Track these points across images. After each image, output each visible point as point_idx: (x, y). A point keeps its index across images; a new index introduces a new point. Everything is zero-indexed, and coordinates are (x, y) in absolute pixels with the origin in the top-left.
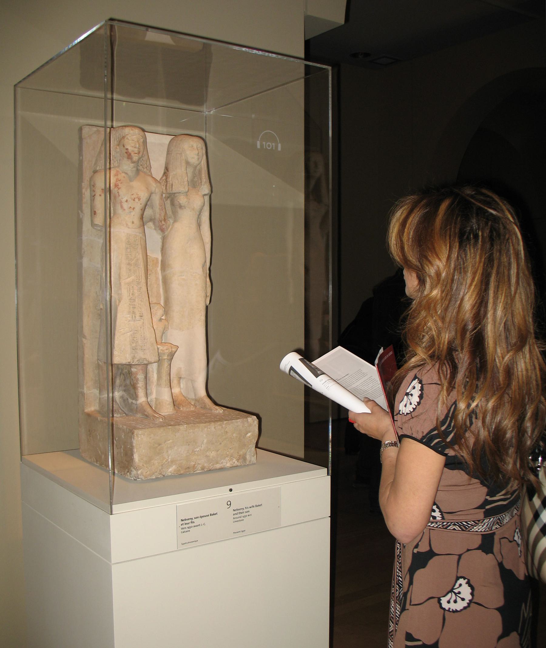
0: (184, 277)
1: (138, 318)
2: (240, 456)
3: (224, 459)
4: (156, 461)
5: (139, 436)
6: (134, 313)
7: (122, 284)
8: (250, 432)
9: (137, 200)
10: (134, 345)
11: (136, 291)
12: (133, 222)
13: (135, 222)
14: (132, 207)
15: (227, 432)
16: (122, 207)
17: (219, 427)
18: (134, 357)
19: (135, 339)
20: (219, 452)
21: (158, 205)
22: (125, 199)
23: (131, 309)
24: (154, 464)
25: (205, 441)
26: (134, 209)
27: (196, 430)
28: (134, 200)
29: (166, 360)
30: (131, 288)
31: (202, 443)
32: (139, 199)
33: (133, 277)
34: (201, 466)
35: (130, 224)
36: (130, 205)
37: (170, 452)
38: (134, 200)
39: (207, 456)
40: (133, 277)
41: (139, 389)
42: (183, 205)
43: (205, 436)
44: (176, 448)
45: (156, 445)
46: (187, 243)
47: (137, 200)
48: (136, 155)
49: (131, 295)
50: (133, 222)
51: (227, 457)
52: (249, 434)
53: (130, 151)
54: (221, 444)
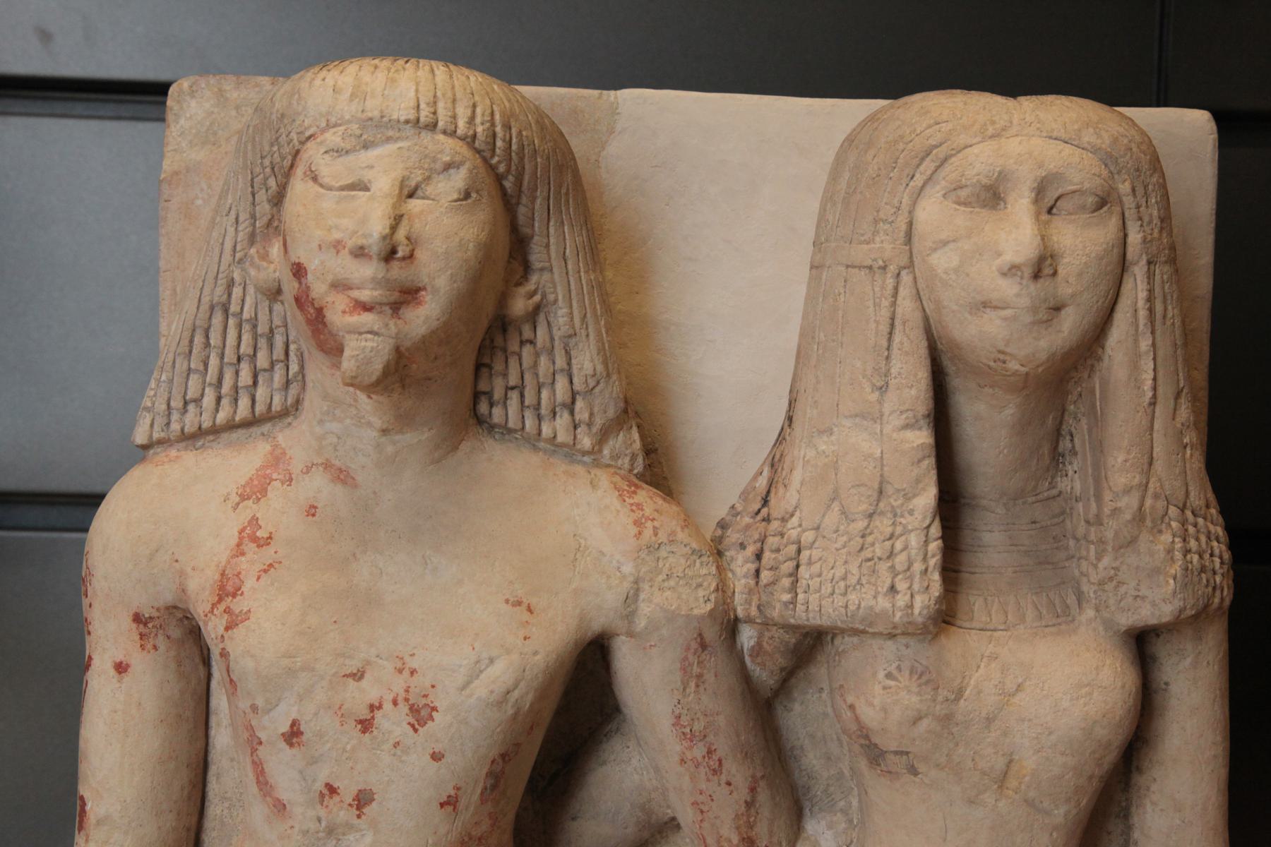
9: (393, 723)
14: (348, 790)
21: (664, 725)
26: (362, 800)
28: (366, 725)
32: (420, 715)
36: (323, 774)
38: (366, 725)
42: (889, 743)
47: (393, 723)
48: (367, 319)
53: (318, 289)
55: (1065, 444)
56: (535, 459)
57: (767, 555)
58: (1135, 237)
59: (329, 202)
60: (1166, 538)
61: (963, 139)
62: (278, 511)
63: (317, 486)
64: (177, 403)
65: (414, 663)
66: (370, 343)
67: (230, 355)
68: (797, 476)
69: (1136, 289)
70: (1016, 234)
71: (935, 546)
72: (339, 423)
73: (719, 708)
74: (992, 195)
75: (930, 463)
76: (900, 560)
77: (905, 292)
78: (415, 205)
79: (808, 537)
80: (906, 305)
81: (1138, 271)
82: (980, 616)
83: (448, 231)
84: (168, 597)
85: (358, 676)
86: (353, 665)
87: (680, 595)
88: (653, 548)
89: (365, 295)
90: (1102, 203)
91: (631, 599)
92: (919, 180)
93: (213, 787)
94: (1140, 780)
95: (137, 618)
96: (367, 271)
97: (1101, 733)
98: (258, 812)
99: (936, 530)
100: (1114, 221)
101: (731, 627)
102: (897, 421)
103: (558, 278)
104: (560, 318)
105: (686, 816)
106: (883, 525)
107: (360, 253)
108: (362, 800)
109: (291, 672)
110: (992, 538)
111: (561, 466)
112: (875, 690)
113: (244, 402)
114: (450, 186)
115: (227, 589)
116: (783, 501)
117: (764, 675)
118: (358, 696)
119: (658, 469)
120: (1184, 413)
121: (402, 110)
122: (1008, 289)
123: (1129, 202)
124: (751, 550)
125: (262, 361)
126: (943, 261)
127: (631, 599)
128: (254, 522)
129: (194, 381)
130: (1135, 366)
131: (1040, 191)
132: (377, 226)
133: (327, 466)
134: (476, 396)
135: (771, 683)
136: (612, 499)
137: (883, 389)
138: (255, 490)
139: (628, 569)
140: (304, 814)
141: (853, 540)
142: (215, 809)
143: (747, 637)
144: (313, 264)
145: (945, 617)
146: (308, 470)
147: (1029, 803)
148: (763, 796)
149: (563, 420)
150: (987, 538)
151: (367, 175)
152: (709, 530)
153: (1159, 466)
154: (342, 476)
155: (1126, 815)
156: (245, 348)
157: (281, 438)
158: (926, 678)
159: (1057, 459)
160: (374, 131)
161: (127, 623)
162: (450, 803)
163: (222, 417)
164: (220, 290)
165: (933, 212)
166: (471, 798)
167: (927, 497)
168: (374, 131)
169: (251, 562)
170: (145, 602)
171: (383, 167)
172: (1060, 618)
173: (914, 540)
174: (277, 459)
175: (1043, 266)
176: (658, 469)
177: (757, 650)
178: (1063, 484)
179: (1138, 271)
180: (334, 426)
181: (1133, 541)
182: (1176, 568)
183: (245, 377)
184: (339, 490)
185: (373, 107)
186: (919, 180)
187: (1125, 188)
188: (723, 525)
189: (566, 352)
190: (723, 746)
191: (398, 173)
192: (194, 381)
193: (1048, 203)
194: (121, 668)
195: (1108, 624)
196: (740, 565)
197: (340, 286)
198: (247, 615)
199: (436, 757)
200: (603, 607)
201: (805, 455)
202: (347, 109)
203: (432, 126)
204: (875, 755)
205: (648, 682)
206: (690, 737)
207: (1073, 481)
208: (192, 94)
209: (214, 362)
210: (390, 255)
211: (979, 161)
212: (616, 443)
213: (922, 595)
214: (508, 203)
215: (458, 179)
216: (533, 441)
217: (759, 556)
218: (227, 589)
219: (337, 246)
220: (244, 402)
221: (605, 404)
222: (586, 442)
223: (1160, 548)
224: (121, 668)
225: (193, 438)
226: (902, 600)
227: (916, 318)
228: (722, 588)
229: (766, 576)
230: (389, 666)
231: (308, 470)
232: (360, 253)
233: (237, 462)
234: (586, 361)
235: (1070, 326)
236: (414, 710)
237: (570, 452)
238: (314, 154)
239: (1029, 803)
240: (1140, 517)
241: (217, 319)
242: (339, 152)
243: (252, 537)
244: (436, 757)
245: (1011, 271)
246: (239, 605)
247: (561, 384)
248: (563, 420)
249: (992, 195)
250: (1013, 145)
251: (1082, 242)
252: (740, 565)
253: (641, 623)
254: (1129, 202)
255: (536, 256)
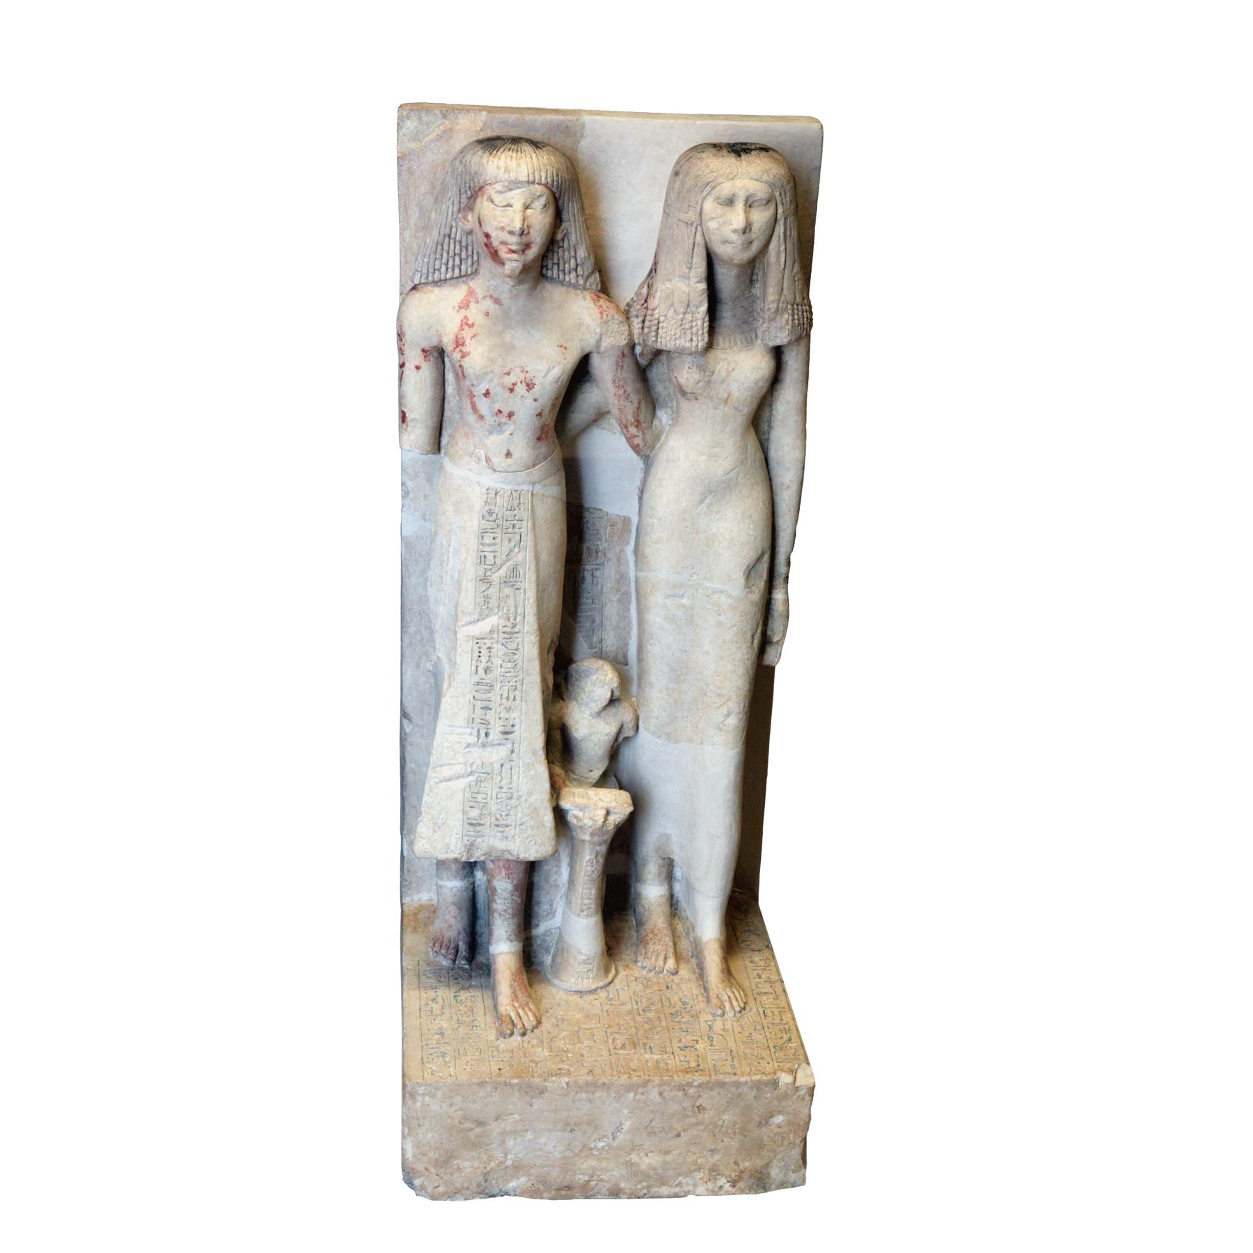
0: (685, 601)
1: (495, 735)
2: (741, 1172)
3: (689, 1173)
4: (467, 1164)
5: (420, 1098)
6: (485, 723)
7: (459, 636)
8: (780, 1112)
9: (521, 389)
10: (474, 813)
11: (497, 662)
12: (508, 454)
13: (516, 455)
14: (506, 411)
15: (700, 1108)
16: (475, 409)
17: (674, 1093)
18: (472, 845)
19: (480, 797)
20: (669, 1158)
22: (482, 389)
23: (478, 711)
24: (459, 1169)
25: (627, 1125)
26: (510, 415)
27: (598, 1094)
28: (512, 390)
29: (587, 845)
30: (484, 652)
31: (619, 1129)
32: (530, 386)
33: (493, 620)
34: (607, 1186)
35: (498, 460)
36: (497, 406)
37: (510, 1143)
38: (512, 390)
39: (630, 1164)
40: (493, 620)
41: (496, 915)
42: (688, 390)
43: (626, 1111)
44: (529, 1135)
45: (468, 1125)
46: (701, 502)
47: (521, 389)
48: (514, 256)
49: (481, 671)
50: (508, 454)
51: (699, 1169)
52: (779, 1119)
53: (495, 244)
54: (678, 1135)
55: (755, 277)
56: (564, 289)
57: (647, 323)
58: (780, 211)
59: (498, 212)
60: (786, 316)
61: (721, 180)
62: (475, 313)
63: (488, 304)
64: (431, 270)
65: (527, 369)
66: (515, 264)
67: (451, 253)
68: (658, 295)
69: (780, 229)
70: (737, 218)
71: (706, 324)
72: (492, 282)
73: (629, 375)
74: (730, 202)
75: (705, 295)
76: (694, 330)
77: (699, 234)
78: (529, 212)
79: (662, 319)
80: (699, 238)
81: (781, 222)
82: (721, 345)
83: (540, 220)
84: (435, 343)
85: (508, 374)
86: (506, 370)
87: (616, 339)
88: (606, 322)
89: (514, 248)
90: (768, 201)
91: (599, 341)
92: (704, 194)
93: (446, 406)
94: (776, 394)
95: (423, 351)
96: (514, 239)
97: (760, 384)
98: (471, 418)
99: (707, 319)
100: (772, 208)
101: (633, 347)
102: (694, 280)
103: (572, 224)
104: (573, 238)
105: (615, 412)
106: (689, 317)
107: (511, 233)
108: (510, 415)
109: (486, 373)
110: (727, 315)
111: (572, 291)
112: (687, 375)
113: (457, 271)
114: (539, 204)
115: (459, 343)
116: (653, 303)
117: (643, 362)
118: (509, 381)
119: (605, 289)
120: (797, 268)
121: (523, 178)
122: (734, 237)
123: (779, 199)
124: (640, 319)
125: (464, 255)
126: (712, 225)
127: (599, 341)
128: (466, 317)
129: (438, 262)
130: (778, 257)
131: (747, 200)
132: (517, 225)
133: (491, 297)
134: (542, 267)
135: (644, 367)
136: (591, 304)
137: (690, 268)
138: (465, 305)
139: (598, 330)
140: (490, 420)
141: (677, 315)
142: (447, 414)
143: (638, 350)
144: (493, 234)
145: (710, 346)
146: (484, 298)
147: (736, 408)
148: (643, 404)
149: (573, 275)
150: (725, 314)
151: (512, 201)
152: (623, 306)
153: (785, 291)
154: (497, 301)
155: (771, 405)
156: (457, 251)
157: (472, 284)
158: (702, 368)
159: (752, 282)
160: (514, 185)
161: (419, 352)
162: (539, 415)
163: (449, 276)
164: (448, 230)
165: (709, 206)
166: (546, 413)
167: (704, 307)
168: (514, 185)
169: (467, 333)
170: (426, 345)
171: (517, 198)
172: (749, 343)
173: (699, 323)
174: (471, 292)
175: (747, 229)
176: (605, 289)
177: (642, 354)
178: (753, 291)
179: (781, 222)
180: (492, 282)
181: (774, 319)
182: (789, 327)
183: (457, 261)
184: (497, 306)
185: (513, 176)
186: (704, 194)
187: (777, 194)
188: (628, 305)
189: (576, 250)
190: (629, 389)
191: (522, 201)
192: (438, 262)
193: (749, 205)
194: (418, 368)
195: (765, 345)
196: (636, 324)
197: (504, 243)
198: (469, 353)
199: (535, 400)
200: (589, 342)
201: (661, 288)
202: (503, 176)
203: (533, 182)
204: (683, 393)
205: (603, 368)
206: (619, 387)
207: (757, 291)
208: (408, 118)
209: (445, 255)
210: (522, 234)
211: (726, 189)
212: (591, 280)
213: (701, 341)
214: (556, 200)
215: (543, 200)
216: (562, 283)
217: (643, 322)
218: (459, 343)
219: (503, 229)
220: (457, 271)
221: (589, 266)
222: (581, 282)
223: (784, 320)
224: (418, 368)
225: (436, 283)
226: (694, 344)
227: (702, 243)
228: (631, 334)
229: (646, 330)
230: (518, 370)
231: (484, 298)
232: (511, 233)
233: (456, 294)
234: (582, 253)
235: (755, 247)
236: (528, 385)
237: (576, 286)
238: (490, 191)
239: (736, 408)
240: (777, 310)
241: (447, 240)
242: (501, 192)
243: (466, 323)
244: (535, 400)
245: (735, 231)
246: (465, 349)
247: (573, 261)
248: (573, 275)
249: (730, 202)
250: (738, 183)
251: (760, 217)
252: (636, 324)
253: (602, 349)
254: (779, 199)
255: (565, 217)
